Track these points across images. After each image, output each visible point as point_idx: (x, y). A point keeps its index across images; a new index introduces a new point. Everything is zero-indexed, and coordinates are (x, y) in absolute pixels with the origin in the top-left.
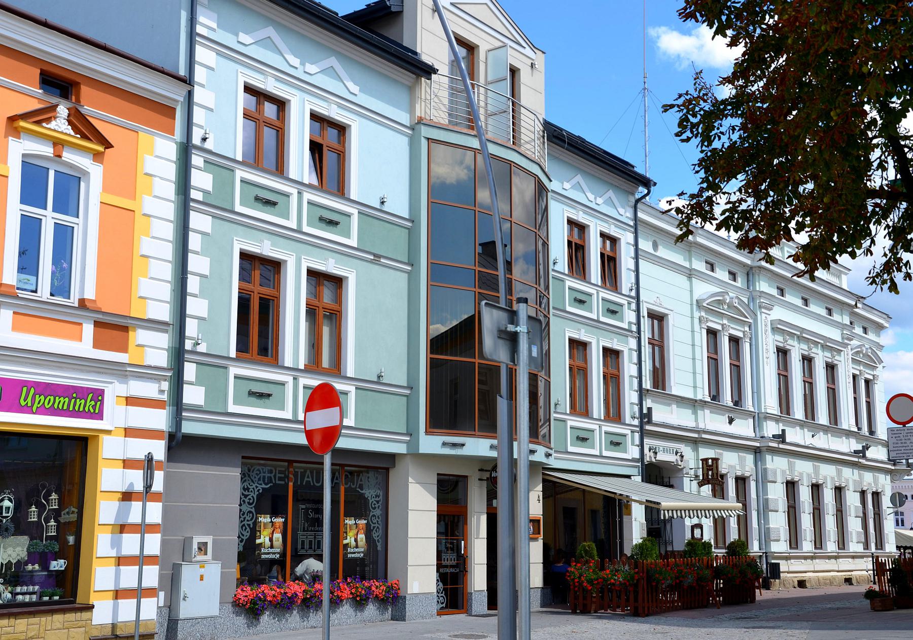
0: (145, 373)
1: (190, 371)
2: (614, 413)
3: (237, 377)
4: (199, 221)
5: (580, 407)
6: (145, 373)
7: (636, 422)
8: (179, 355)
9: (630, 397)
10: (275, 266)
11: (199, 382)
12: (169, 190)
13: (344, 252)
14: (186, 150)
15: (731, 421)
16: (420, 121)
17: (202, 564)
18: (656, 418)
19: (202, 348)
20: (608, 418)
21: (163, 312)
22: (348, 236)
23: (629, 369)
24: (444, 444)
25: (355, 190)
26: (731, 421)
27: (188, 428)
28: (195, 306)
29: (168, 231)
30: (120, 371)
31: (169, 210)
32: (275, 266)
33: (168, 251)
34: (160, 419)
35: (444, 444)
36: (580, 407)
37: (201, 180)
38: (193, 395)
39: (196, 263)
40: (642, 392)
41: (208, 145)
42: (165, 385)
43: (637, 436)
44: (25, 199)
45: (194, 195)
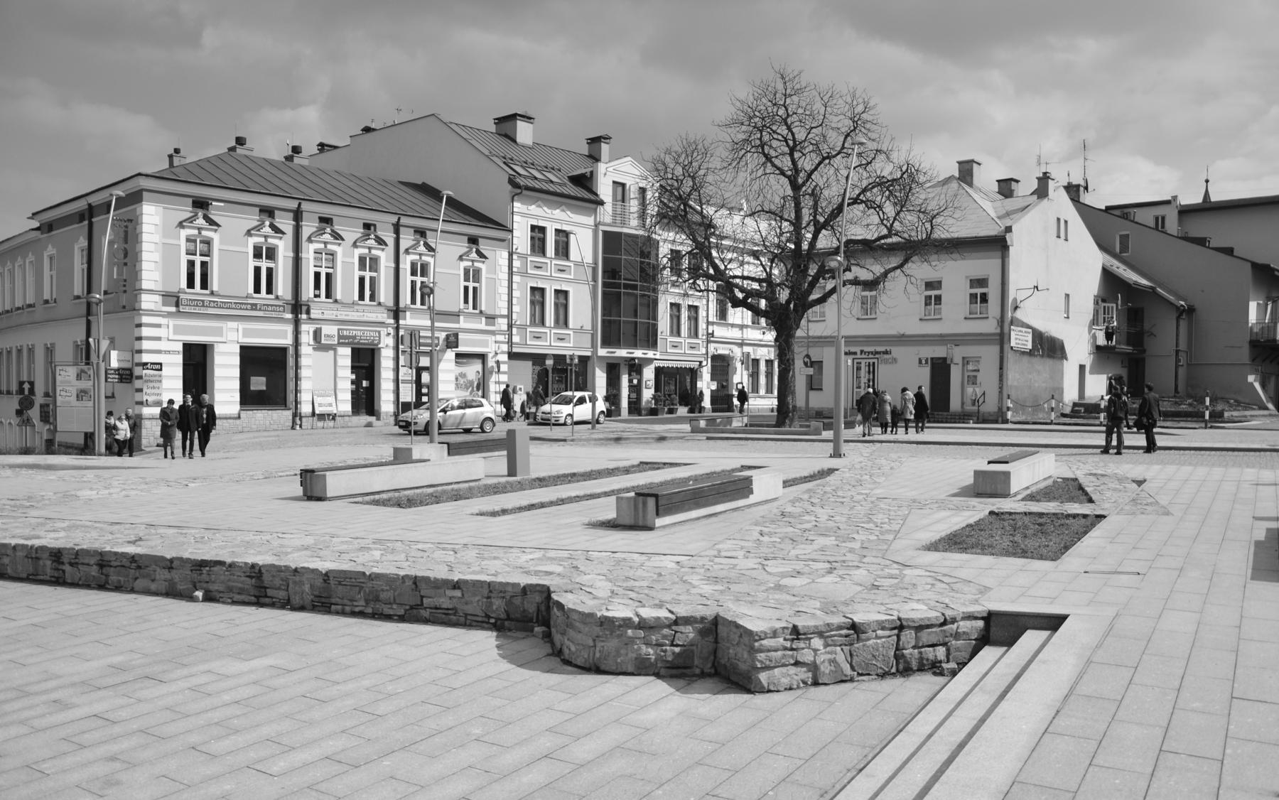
0: (501, 332)
1: (514, 330)
2: (695, 333)
3: (530, 332)
4: (516, 278)
5: (676, 331)
6: (501, 332)
7: (704, 337)
8: (510, 326)
9: (702, 325)
10: (542, 291)
11: (517, 334)
12: (506, 269)
13: (568, 281)
14: (511, 255)
15: (764, 333)
16: (599, 223)
17: (520, 395)
18: (715, 334)
19: (518, 323)
20: (690, 336)
21: (505, 312)
22: (570, 274)
23: (702, 313)
24: (608, 352)
25: (572, 258)
26: (764, 333)
27: (515, 350)
28: (516, 309)
29: (506, 283)
30: (493, 333)
31: (506, 276)
32: (542, 291)
33: (506, 290)
34: (505, 348)
35: (608, 352)
36: (676, 331)
37: (516, 263)
38: (516, 339)
39: (516, 294)
40: (708, 323)
41: (518, 251)
42: (507, 336)
43: (705, 343)
44: (465, 281)
45: (514, 270)
